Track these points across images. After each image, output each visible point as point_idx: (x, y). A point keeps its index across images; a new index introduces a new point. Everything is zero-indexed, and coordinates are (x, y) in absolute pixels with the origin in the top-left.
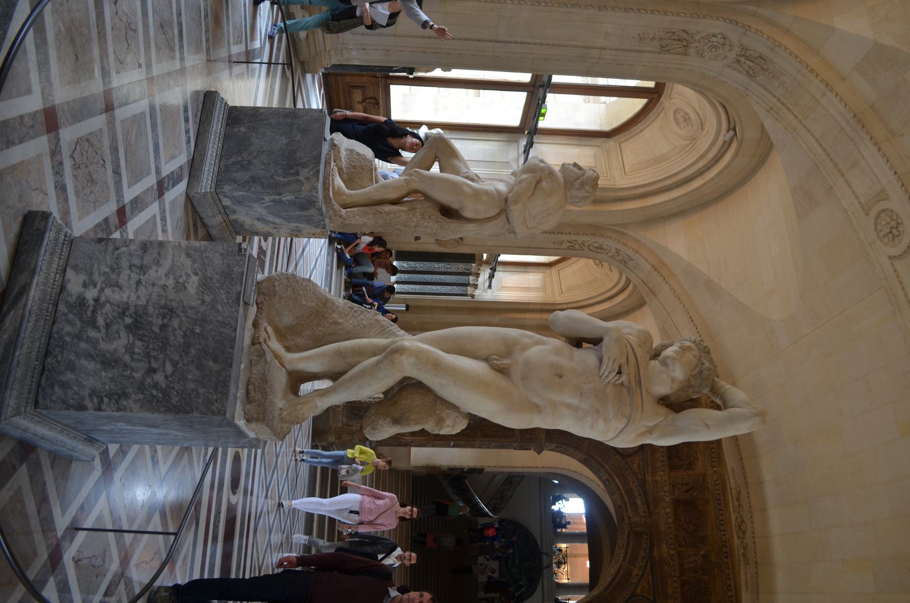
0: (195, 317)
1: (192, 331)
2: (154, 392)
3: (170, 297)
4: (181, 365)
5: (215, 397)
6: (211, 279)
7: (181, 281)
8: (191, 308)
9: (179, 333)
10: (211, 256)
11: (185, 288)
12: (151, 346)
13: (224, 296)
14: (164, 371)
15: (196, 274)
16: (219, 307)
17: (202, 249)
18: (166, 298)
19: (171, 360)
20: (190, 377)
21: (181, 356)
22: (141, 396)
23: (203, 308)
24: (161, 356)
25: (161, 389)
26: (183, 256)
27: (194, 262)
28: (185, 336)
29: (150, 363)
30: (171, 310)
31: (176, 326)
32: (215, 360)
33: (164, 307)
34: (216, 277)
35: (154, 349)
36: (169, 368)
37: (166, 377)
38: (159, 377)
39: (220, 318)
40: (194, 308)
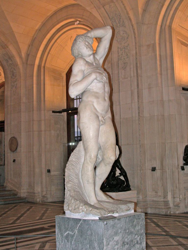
0: (124, 233)
1: (128, 232)
2: (141, 239)
3: (120, 245)
4: (135, 233)
5: (141, 218)
6: (115, 232)
7: (116, 244)
8: (122, 236)
9: (129, 237)
10: (108, 235)
11: (117, 241)
12: (132, 245)
13: (119, 225)
14: (137, 238)
15: (114, 238)
16: (122, 226)
17: (106, 240)
18: (120, 247)
19: (134, 237)
20: (138, 229)
21: (133, 234)
22: (142, 243)
23: (122, 232)
24: (134, 241)
25: (141, 237)
26: (109, 246)
27: (110, 241)
28: (129, 235)
29: (135, 244)
30: (123, 243)
31: (127, 239)
32: (134, 222)
33: (123, 246)
34: (114, 230)
35: (132, 244)
36: (137, 236)
37: (138, 236)
38: (138, 239)
39: (124, 224)
40: (122, 235)
